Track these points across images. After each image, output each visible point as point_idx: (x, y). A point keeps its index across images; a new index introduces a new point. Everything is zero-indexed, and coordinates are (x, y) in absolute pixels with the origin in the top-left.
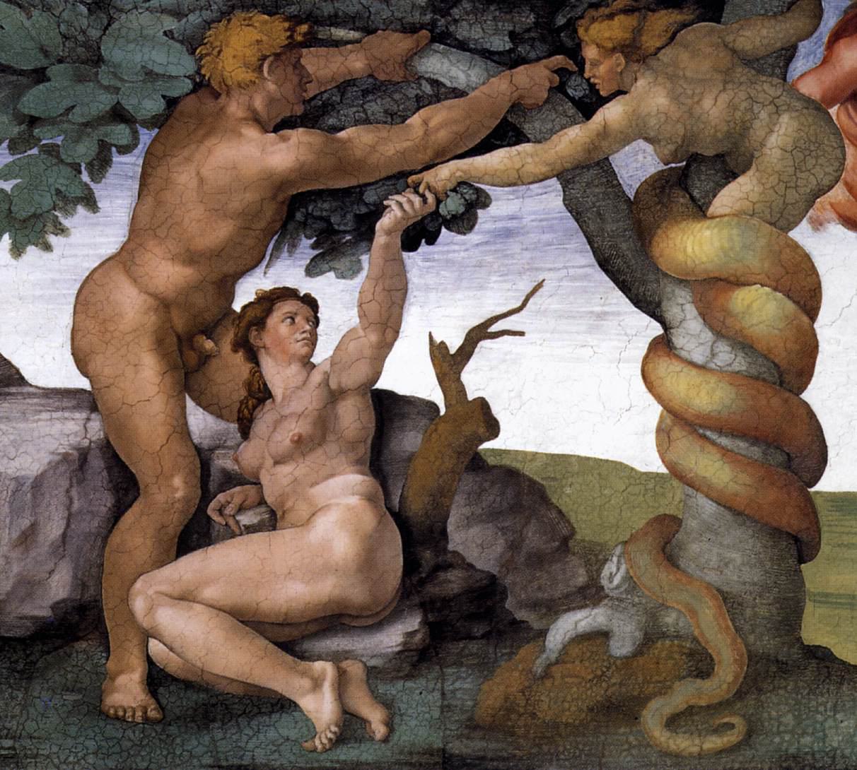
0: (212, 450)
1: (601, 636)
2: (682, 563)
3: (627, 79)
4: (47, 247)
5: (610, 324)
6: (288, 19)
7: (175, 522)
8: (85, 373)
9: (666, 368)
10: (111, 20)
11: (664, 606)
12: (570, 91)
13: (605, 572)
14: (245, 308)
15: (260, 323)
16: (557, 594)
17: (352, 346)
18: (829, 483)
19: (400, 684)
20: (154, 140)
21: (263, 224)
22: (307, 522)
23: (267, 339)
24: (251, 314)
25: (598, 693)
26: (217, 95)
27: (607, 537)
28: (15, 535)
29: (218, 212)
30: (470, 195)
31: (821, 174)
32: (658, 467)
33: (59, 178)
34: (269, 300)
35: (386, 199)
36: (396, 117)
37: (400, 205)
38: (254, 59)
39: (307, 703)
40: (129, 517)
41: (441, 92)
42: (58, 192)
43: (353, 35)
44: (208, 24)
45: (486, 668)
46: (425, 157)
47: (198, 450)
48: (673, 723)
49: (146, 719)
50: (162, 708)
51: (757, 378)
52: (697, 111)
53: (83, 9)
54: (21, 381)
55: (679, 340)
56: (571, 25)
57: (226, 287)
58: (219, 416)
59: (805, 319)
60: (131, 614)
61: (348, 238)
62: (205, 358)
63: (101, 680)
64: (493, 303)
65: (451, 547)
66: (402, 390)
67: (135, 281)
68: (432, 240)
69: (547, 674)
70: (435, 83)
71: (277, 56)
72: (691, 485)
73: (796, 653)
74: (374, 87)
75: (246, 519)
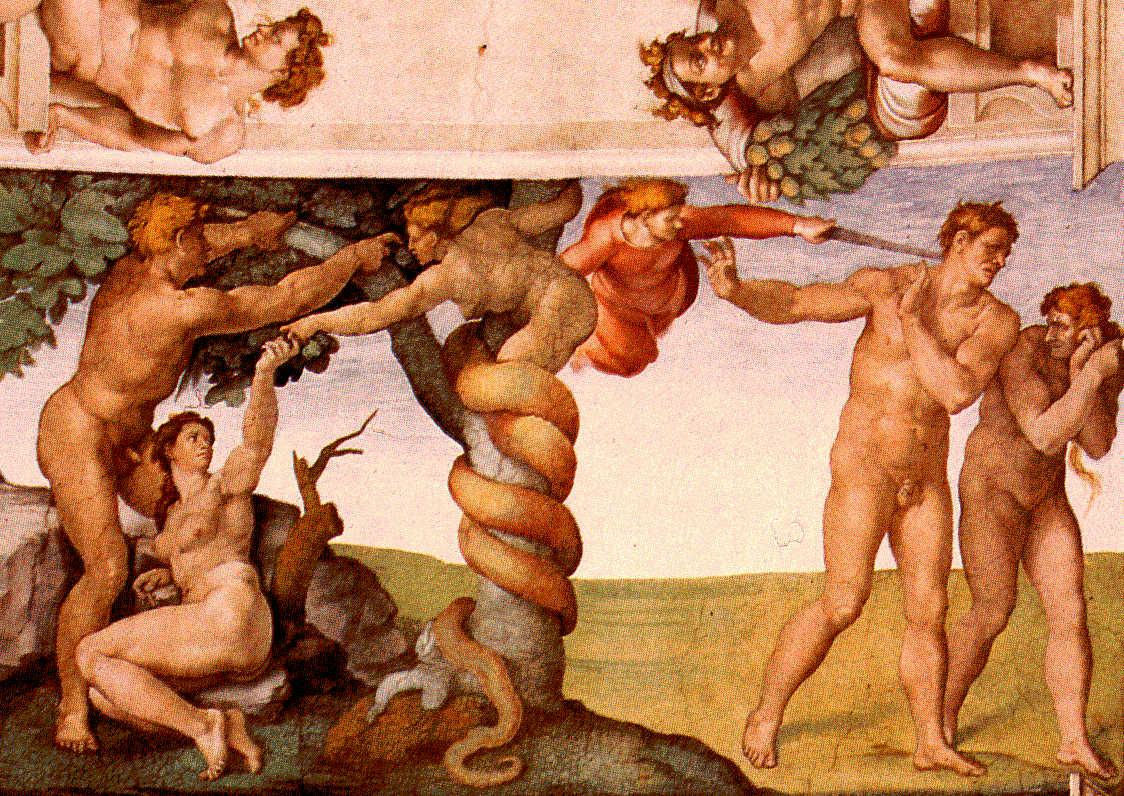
2: (476, 635)
17: (238, 461)
30: (324, 342)
31: (579, 327)
35: (264, 344)
37: (273, 349)
46: (290, 312)
51: (532, 489)
55: (475, 457)
56: (400, 209)
59: (567, 442)
66: (273, 495)
73: (557, 707)
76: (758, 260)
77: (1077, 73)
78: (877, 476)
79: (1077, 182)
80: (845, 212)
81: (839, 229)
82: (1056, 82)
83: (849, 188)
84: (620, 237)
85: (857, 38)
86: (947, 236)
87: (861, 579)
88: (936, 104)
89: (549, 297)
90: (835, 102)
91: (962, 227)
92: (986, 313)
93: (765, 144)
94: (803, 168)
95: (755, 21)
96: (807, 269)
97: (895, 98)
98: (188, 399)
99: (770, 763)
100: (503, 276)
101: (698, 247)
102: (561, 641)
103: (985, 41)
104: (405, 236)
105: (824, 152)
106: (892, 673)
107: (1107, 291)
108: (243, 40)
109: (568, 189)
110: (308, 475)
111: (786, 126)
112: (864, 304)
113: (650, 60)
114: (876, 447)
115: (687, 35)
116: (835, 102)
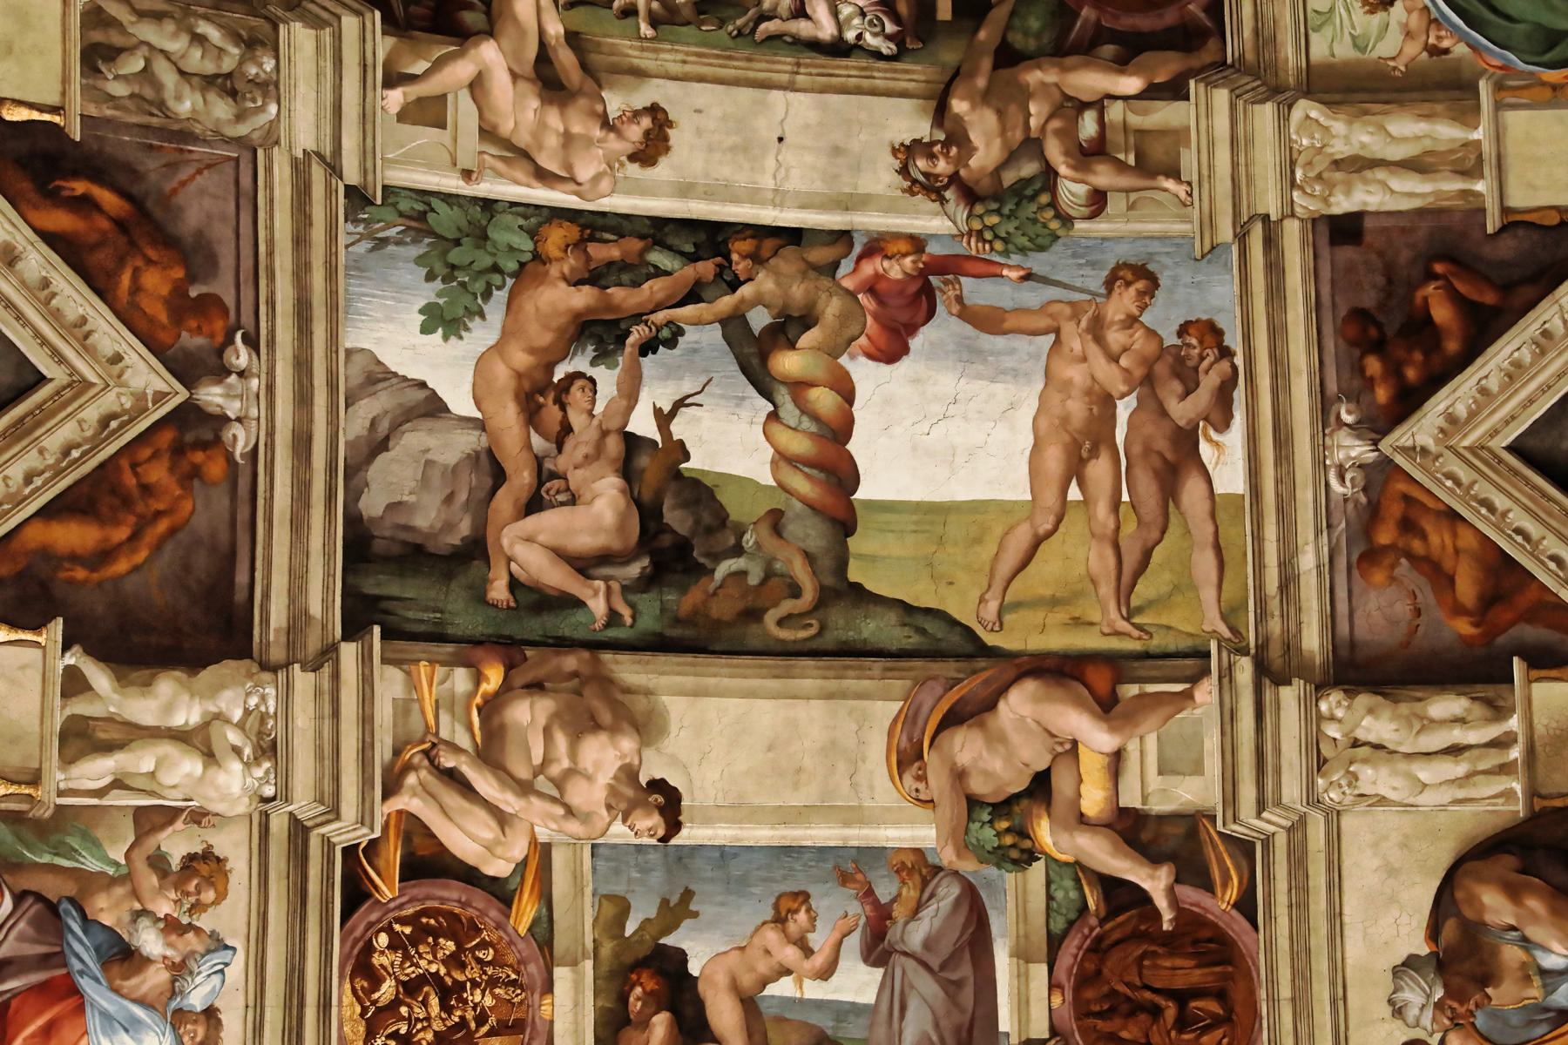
0: (544, 458)
1: (742, 574)
2: (785, 535)
3: (754, 272)
4: (461, 338)
5: (747, 403)
6: (579, 226)
7: (525, 496)
8: (479, 409)
9: (776, 429)
10: (492, 217)
11: (775, 559)
13: (745, 539)
15: (567, 390)
18: (860, 495)
21: (568, 336)
23: (570, 399)
25: (740, 605)
26: (545, 264)
27: (745, 519)
28: (443, 497)
29: (546, 327)
31: (854, 329)
33: (466, 300)
36: (636, 284)
38: (563, 246)
39: (591, 603)
40: (501, 492)
41: (659, 273)
42: (466, 308)
43: (615, 238)
44: (540, 225)
45: (684, 590)
46: (651, 307)
47: (536, 457)
48: (781, 623)
49: (509, 607)
50: (516, 601)
51: (822, 436)
54: (447, 410)
55: (782, 414)
56: (725, 242)
57: (549, 368)
58: (546, 438)
60: (501, 547)
62: (540, 407)
64: (687, 387)
66: (639, 433)
68: (654, 352)
69: (715, 594)
70: (656, 267)
71: (576, 245)
75: (561, 498)
76: (978, 291)
77: (1195, 185)
78: (1067, 438)
79: (1198, 256)
80: (1038, 262)
82: (1181, 190)
83: (1041, 249)
85: (1042, 152)
86: (1110, 283)
87: (1058, 504)
88: (1098, 201)
89: (831, 308)
90: (1029, 192)
91: (1121, 278)
92: (1139, 334)
93: (981, 217)
94: (1008, 233)
95: (972, 137)
98: (580, 362)
99: (997, 628)
100: (798, 292)
101: (935, 280)
103: (1131, 160)
104: (730, 262)
107: (1222, 323)
109: (843, 237)
110: (664, 419)
111: (994, 206)
112: (1055, 324)
113: (900, 156)
114: (1065, 420)
116: (1029, 192)
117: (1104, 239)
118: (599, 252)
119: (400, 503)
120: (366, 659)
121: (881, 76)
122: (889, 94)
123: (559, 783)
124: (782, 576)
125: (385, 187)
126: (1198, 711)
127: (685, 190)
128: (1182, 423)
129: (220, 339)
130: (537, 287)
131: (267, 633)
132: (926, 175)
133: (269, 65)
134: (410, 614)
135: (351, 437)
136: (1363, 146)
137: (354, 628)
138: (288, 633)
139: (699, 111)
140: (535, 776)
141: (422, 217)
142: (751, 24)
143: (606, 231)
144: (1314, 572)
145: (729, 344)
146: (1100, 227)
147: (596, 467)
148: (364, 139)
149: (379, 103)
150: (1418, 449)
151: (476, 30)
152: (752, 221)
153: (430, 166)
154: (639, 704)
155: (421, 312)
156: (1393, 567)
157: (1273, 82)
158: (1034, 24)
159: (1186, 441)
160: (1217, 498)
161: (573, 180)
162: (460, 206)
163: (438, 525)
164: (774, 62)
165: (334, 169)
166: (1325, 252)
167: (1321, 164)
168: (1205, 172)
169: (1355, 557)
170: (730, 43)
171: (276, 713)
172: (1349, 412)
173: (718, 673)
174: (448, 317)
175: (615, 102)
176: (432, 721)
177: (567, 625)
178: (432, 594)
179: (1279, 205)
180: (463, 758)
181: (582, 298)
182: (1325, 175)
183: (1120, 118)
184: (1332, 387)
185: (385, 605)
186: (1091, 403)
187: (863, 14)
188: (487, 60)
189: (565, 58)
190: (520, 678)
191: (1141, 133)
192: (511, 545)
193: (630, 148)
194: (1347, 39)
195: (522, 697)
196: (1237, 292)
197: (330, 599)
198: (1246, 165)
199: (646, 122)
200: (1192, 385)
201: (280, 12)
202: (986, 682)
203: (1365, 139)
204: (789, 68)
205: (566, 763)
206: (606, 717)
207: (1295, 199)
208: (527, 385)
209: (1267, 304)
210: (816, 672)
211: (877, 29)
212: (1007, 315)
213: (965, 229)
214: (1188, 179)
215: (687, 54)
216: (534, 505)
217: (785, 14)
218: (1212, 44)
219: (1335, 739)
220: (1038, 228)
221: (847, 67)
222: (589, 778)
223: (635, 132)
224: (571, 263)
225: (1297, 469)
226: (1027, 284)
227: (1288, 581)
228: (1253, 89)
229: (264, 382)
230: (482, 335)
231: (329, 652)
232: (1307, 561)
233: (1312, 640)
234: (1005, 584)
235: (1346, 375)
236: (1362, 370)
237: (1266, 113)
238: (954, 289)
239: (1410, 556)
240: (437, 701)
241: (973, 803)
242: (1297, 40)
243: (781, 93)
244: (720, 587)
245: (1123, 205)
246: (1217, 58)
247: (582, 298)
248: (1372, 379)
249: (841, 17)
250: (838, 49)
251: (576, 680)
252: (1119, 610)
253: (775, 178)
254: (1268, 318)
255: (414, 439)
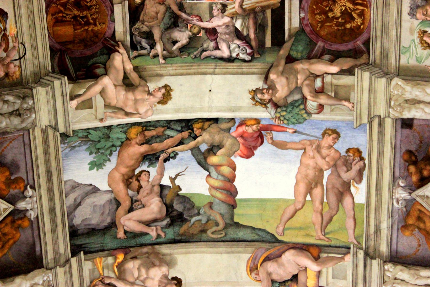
0: (133, 197)
1: (200, 220)
2: (213, 209)
3: (202, 133)
4: (103, 169)
6: (142, 126)
7: (127, 208)
9: (210, 179)
12: (192, 136)
13: (201, 210)
14: (137, 174)
15: (140, 176)
16: (192, 214)
18: (238, 197)
19: (166, 229)
20: (120, 149)
22: (150, 206)
24: (138, 175)
25: (200, 229)
26: (130, 140)
27: (200, 205)
28: (101, 214)
30: (175, 153)
32: (209, 194)
33: (104, 157)
34: (141, 172)
36: (161, 141)
37: (163, 155)
38: (136, 134)
39: (151, 233)
41: (169, 137)
42: (104, 160)
43: (154, 128)
44: (128, 129)
45: (181, 226)
46: (167, 148)
47: (131, 197)
48: (213, 233)
49: (124, 239)
50: (127, 236)
51: (225, 181)
52: (214, 138)
53: (106, 129)
54: (100, 190)
55: (212, 175)
56: (192, 125)
57: (134, 170)
58: (134, 191)
59: (234, 172)
60: (121, 223)
61: (154, 161)
62: (131, 183)
63: (116, 233)
64: (179, 170)
65: (174, 208)
66: (165, 184)
67: (118, 172)
68: (169, 160)
69: (191, 226)
70: (168, 135)
71: (140, 133)
72: (215, 197)
73: (233, 223)
74: (157, 137)
75: (139, 207)
76: (279, 136)
78: (307, 181)
79: (355, 126)
80: (299, 127)
81: (298, 131)
82: (350, 106)
83: (300, 123)
84: (245, 130)
85: (302, 92)
86: (324, 135)
88: (321, 107)
89: (228, 142)
90: (297, 104)
92: (333, 151)
93: (280, 112)
94: (289, 118)
95: (277, 86)
96: (290, 139)
97: (311, 104)
98: (144, 167)
99: (282, 235)
100: (217, 138)
101: (263, 132)
102: (233, 211)
103: (333, 95)
105: (294, 115)
106: (311, 221)
107: (361, 149)
108: (152, 92)
109: (232, 120)
110: (173, 180)
111: (284, 109)
112: (304, 147)
113: (251, 94)
114: (307, 176)
115: (260, 88)
116: (297, 104)
117: (322, 121)
118: (148, 134)
119: (86, 219)
120: (79, 261)
121: (245, 67)
122: (248, 74)
123: (143, 281)
124: (213, 220)
125: (73, 131)
126: (346, 263)
127: (177, 111)
128: (345, 180)
129: (22, 189)
130: (128, 148)
131: (48, 261)
132: (261, 99)
133: (31, 102)
134: (93, 246)
135: (68, 204)
136: (416, 96)
137: (74, 253)
138: (54, 259)
139: (182, 85)
140: (136, 280)
141: (87, 137)
142: (200, 53)
143: (150, 127)
144: (386, 229)
145: (194, 156)
146: (321, 117)
147: (151, 196)
148: (65, 117)
149: (69, 105)
150: (425, 196)
151: (101, 75)
152: (201, 118)
153: (89, 121)
154: (168, 258)
155: (89, 164)
156: (412, 231)
157: (385, 71)
158: (300, 48)
159: (347, 186)
160: (355, 204)
161: (138, 113)
162: (99, 130)
163: (99, 221)
164: (207, 66)
165: (55, 129)
166: (399, 130)
167: (401, 101)
168: (359, 100)
169: (400, 227)
170: (193, 61)
171: (53, 280)
172: (402, 183)
173: (191, 247)
174: (98, 163)
175: (152, 86)
176: (101, 272)
177: (145, 240)
178: (100, 240)
179: (385, 113)
180: (112, 280)
181: (144, 149)
182: (402, 105)
183: (330, 81)
184: (397, 174)
185: (84, 246)
186: (316, 171)
187: (239, 47)
188: (106, 83)
189: (134, 76)
190: (129, 256)
191: (336, 86)
192: (124, 222)
193: (158, 100)
194: (414, 58)
195: (129, 261)
196: (368, 139)
197: (66, 248)
198: (374, 99)
199: (163, 91)
200: (350, 168)
201: (33, 85)
202: (279, 250)
203: (418, 93)
204: (213, 67)
205: (145, 276)
206: (157, 263)
207: (390, 111)
208: (126, 177)
209: (378, 144)
210: (224, 246)
211: (244, 52)
212: (288, 144)
213: (274, 116)
214: (353, 102)
215: (177, 67)
216: (131, 210)
217: (211, 49)
218: (365, 56)
219: (389, 276)
220: (299, 116)
221: (233, 66)
222: (153, 279)
223: (159, 95)
224: (139, 139)
225: (383, 198)
226: (295, 134)
227: (377, 231)
228: (378, 73)
229: (38, 198)
230: (110, 166)
231: (68, 261)
232: (384, 226)
233: (384, 248)
234: (285, 222)
235: (403, 171)
236: (408, 170)
237: (383, 81)
238: (270, 135)
239: (419, 228)
240: (103, 268)
241: (273, 281)
242: (396, 57)
243: (210, 75)
244: (193, 224)
245: (329, 110)
246: (366, 61)
247: (144, 149)
248: (411, 173)
249: (231, 49)
250: (230, 60)
251: (147, 255)
252: (322, 233)
253: (208, 103)
254: (378, 149)
255: (90, 200)
